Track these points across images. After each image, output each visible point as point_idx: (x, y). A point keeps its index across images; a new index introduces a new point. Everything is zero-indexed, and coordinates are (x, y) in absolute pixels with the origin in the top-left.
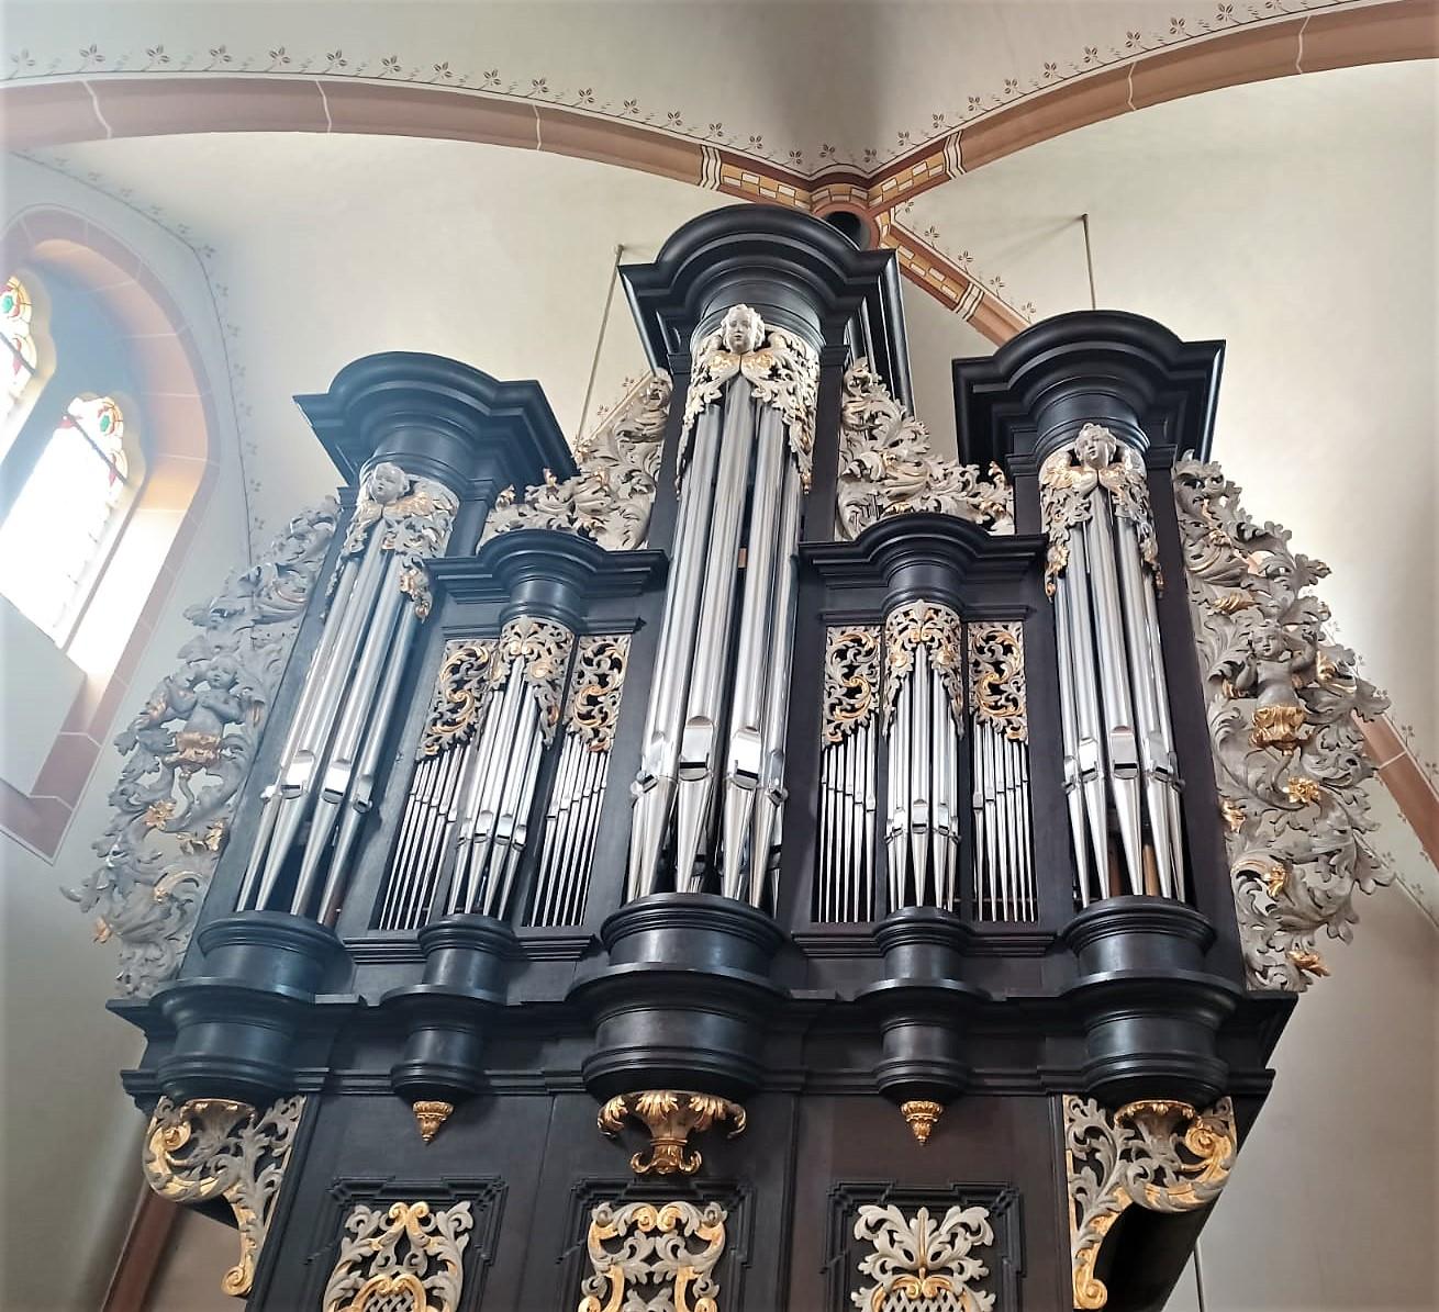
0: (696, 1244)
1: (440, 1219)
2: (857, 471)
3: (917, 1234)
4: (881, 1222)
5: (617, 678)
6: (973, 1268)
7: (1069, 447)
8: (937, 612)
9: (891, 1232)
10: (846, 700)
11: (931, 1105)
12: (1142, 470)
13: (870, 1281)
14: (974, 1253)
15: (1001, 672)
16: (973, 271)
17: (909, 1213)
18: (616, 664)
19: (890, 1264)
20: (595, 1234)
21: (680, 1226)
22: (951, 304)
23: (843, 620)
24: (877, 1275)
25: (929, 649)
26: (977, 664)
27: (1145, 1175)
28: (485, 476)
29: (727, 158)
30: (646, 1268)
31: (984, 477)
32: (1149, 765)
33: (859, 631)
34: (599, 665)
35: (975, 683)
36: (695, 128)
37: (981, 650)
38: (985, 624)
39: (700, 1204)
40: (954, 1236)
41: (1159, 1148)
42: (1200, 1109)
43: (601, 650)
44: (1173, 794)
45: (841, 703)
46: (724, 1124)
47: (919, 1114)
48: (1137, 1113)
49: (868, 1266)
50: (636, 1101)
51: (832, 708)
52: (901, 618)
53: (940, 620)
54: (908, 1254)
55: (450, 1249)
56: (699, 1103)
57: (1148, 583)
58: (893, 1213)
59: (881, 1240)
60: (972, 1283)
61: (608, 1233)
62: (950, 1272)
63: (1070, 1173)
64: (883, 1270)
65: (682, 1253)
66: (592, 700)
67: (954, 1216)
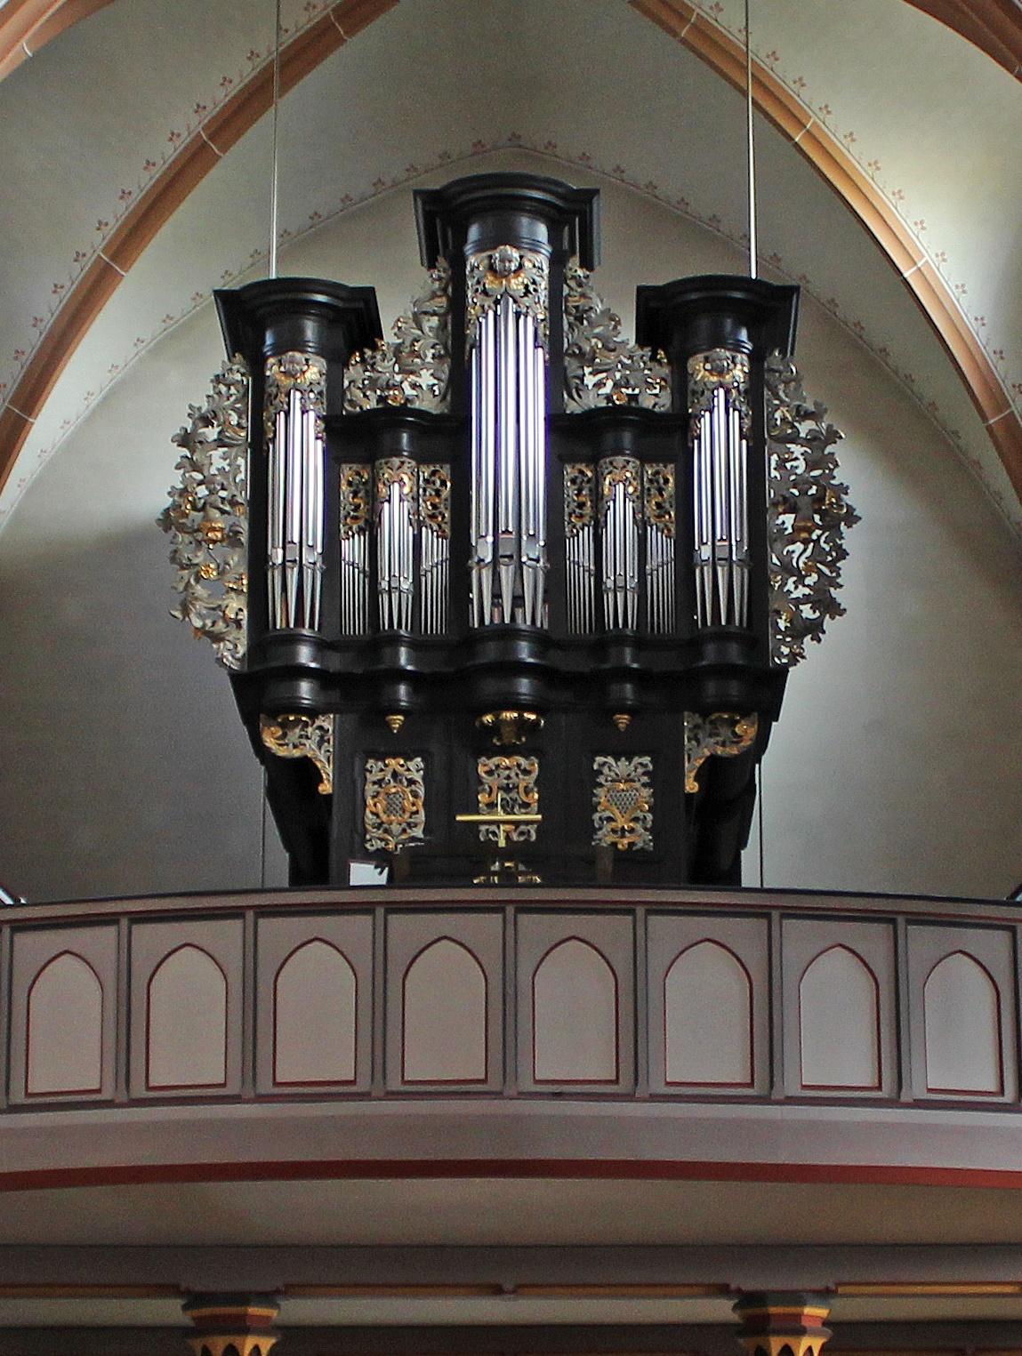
0: (526, 772)
1: (411, 765)
2: (577, 352)
3: (623, 767)
4: (605, 763)
5: (446, 493)
6: (645, 779)
7: (707, 354)
8: (628, 462)
9: (609, 768)
10: (577, 510)
11: (626, 717)
12: (746, 369)
13: (601, 785)
14: (644, 774)
15: (662, 495)
17: (617, 759)
18: (443, 483)
19: (609, 779)
20: (481, 770)
21: (519, 766)
23: (573, 460)
24: (603, 782)
25: (624, 485)
26: (649, 489)
27: (717, 743)
28: (339, 341)
30: (506, 782)
31: (653, 358)
32: (734, 558)
33: (583, 467)
34: (434, 483)
35: (648, 502)
37: (651, 481)
38: (654, 465)
39: (527, 758)
40: (636, 768)
41: (725, 732)
42: (743, 716)
43: (434, 473)
44: (746, 571)
45: (574, 512)
46: (536, 723)
47: (623, 720)
48: (716, 719)
49: (601, 779)
50: (499, 715)
51: (570, 515)
52: (608, 465)
53: (630, 466)
54: (616, 774)
55: (418, 777)
56: (526, 715)
57: (744, 442)
58: (610, 760)
59: (606, 770)
60: (644, 785)
61: (486, 769)
62: (634, 781)
63: (686, 743)
64: (606, 781)
65: (521, 776)
66: (434, 506)
67: (636, 760)
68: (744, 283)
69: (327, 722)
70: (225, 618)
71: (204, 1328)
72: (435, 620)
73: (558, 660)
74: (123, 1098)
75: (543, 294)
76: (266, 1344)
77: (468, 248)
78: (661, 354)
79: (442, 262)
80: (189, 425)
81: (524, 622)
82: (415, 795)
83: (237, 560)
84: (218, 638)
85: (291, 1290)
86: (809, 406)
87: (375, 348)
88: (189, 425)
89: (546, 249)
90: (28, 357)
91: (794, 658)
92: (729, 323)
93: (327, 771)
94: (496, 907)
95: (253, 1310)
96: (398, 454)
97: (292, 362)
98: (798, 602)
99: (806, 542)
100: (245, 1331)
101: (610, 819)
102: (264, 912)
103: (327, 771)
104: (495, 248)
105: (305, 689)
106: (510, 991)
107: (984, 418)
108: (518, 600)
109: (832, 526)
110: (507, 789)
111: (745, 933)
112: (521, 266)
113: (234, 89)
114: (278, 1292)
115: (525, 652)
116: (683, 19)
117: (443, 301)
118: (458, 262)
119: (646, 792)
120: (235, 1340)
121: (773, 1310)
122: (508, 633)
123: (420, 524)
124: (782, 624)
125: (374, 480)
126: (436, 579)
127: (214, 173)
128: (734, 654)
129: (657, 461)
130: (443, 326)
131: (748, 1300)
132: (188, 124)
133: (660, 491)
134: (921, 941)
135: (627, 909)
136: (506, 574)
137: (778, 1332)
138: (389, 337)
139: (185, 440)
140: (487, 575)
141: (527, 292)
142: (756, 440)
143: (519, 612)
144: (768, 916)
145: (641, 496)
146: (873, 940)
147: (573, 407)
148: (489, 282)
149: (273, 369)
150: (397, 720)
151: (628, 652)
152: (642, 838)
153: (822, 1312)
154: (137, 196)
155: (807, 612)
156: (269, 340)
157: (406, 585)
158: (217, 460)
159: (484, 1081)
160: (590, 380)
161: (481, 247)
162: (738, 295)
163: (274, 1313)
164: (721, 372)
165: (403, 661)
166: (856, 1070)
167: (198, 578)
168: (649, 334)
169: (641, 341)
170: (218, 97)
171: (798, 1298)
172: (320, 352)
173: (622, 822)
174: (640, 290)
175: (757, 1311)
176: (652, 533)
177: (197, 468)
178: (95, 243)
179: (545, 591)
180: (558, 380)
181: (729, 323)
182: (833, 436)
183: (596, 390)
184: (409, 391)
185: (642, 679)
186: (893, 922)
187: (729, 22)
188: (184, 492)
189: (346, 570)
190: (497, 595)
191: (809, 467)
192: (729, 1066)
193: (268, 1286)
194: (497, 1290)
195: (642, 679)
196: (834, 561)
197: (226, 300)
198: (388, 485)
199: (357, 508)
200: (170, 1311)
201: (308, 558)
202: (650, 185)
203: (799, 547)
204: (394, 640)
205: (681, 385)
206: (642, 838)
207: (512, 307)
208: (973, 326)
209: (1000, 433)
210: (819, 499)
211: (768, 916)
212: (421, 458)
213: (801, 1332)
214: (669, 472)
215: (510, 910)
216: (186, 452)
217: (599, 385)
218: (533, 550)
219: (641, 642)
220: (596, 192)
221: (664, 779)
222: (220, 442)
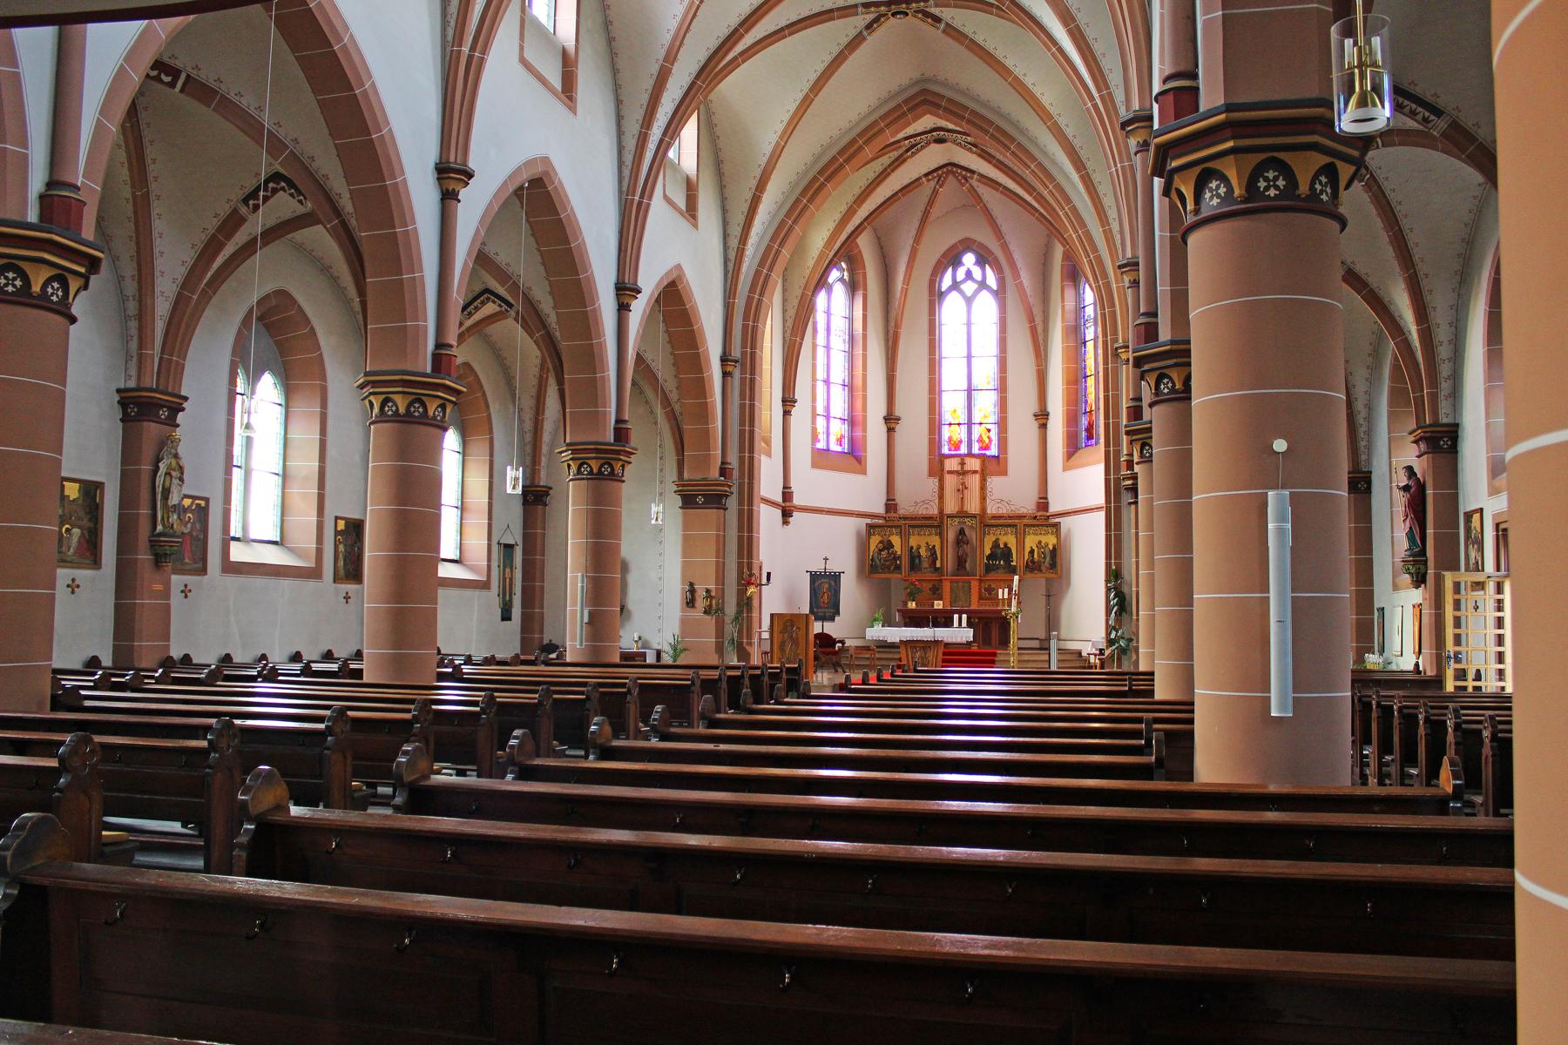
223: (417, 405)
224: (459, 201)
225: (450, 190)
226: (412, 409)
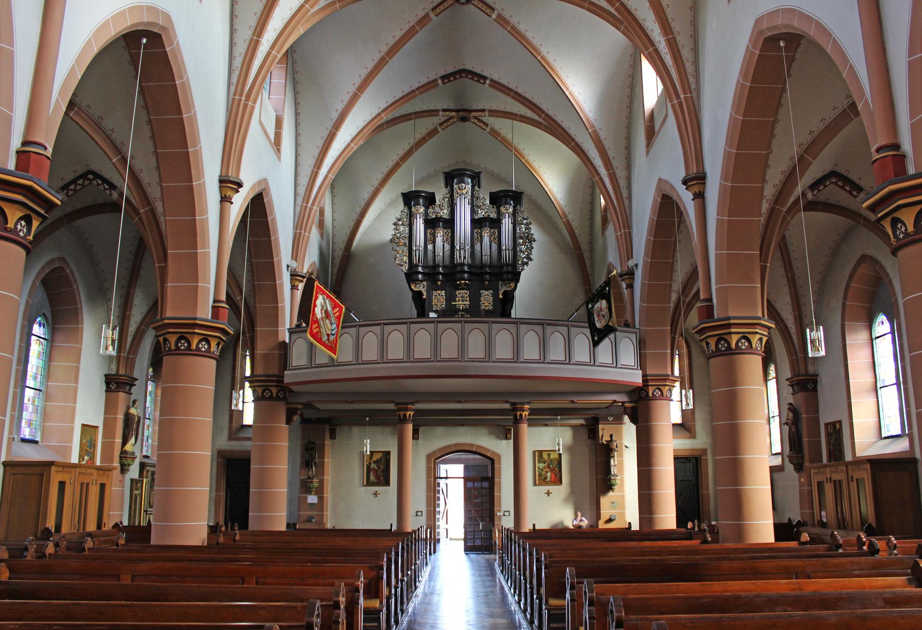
0: (466, 294)
3: (486, 292)
5: (449, 235)
16: (489, 122)
18: (449, 233)
20: (457, 293)
22: (485, 130)
23: (476, 228)
28: (427, 203)
29: (444, 110)
31: (493, 207)
36: (439, 106)
41: (508, 285)
47: (487, 283)
55: (444, 295)
68: (512, 191)
69: (425, 283)
70: (403, 261)
71: (399, 410)
72: (447, 262)
73: (473, 270)
74: (382, 362)
75: (470, 194)
76: (412, 413)
77: (454, 184)
78: (495, 206)
79: (449, 187)
80: (396, 221)
81: (466, 262)
82: (443, 298)
83: (406, 249)
84: (402, 265)
85: (417, 402)
86: (526, 217)
87: (435, 205)
88: (396, 221)
89: (470, 184)
90: (362, 207)
91: (523, 270)
92: (509, 200)
93: (425, 293)
94: (460, 322)
95: (409, 406)
96: (440, 227)
97: (417, 208)
98: (523, 258)
99: (525, 245)
100: (408, 411)
101: (484, 303)
102: (411, 323)
103: (425, 293)
104: (460, 184)
105: (420, 276)
106: (463, 339)
107: (562, 220)
108: (465, 258)
109: (530, 242)
110: (462, 297)
111: (512, 327)
112: (465, 188)
113: (405, 151)
114: (414, 402)
115: (466, 269)
116: (499, 136)
117: (449, 195)
118: (452, 187)
119: (491, 298)
120: (406, 412)
121: (518, 406)
122: (462, 265)
123: (444, 242)
124: (520, 263)
125: (435, 232)
126: (447, 253)
127: (401, 168)
128: (510, 269)
129: (494, 228)
130: (449, 200)
131: (513, 404)
132: (396, 158)
133: (494, 235)
134: (549, 329)
135: (487, 322)
136: (462, 252)
137: (519, 411)
138: (438, 203)
139: (395, 224)
140: (458, 252)
141: (467, 193)
142: (514, 224)
143: (465, 260)
144: (517, 324)
145: (490, 236)
146: (539, 329)
147: (476, 217)
148: (459, 191)
149: (413, 209)
150: (439, 283)
151: (488, 269)
152: (491, 307)
153: (529, 407)
154: (385, 173)
155: (525, 260)
156: (412, 203)
157: (441, 255)
158: (402, 228)
159: (458, 358)
160: (480, 212)
161: (457, 183)
162: (511, 194)
163: (413, 407)
164: (507, 210)
165: (441, 270)
166: (536, 356)
167: (398, 253)
168: (492, 202)
169: (490, 203)
170: (402, 152)
171: (523, 404)
172: (423, 206)
173: (486, 304)
174: (490, 193)
175: (515, 406)
176: (493, 244)
177: (397, 230)
178: (376, 183)
179: (470, 256)
180: (473, 212)
181: (509, 200)
182: (530, 223)
183: (481, 214)
184: (442, 214)
185: (490, 274)
186: (543, 325)
187: (509, 137)
188: (395, 235)
189: (429, 251)
190: (460, 257)
191: (526, 230)
192: (509, 355)
193: (412, 401)
194: (460, 402)
195: (490, 274)
196: (531, 249)
197: (404, 195)
198: (437, 233)
199: (431, 238)
200: (392, 406)
201: (421, 249)
202: (492, 171)
203: (523, 246)
204: (439, 266)
205: (499, 212)
206: (491, 307)
207: (463, 196)
208: (560, 200)
209: (565, 223)
210: (528, 236)
211: (517, 324)
212: (444, 228)
213: (524, 411)
214: (496, 231)
215: (463, 322)
216: (395, 227)
217: (482, 213)
218: (468, 247)
219: (491, 266)
220: (481, 172)
221: (495, 295)
222: (402, 225)
223: (204, 343)
224: (232, 203)
225: (227, 196)
226: (200, 346)
